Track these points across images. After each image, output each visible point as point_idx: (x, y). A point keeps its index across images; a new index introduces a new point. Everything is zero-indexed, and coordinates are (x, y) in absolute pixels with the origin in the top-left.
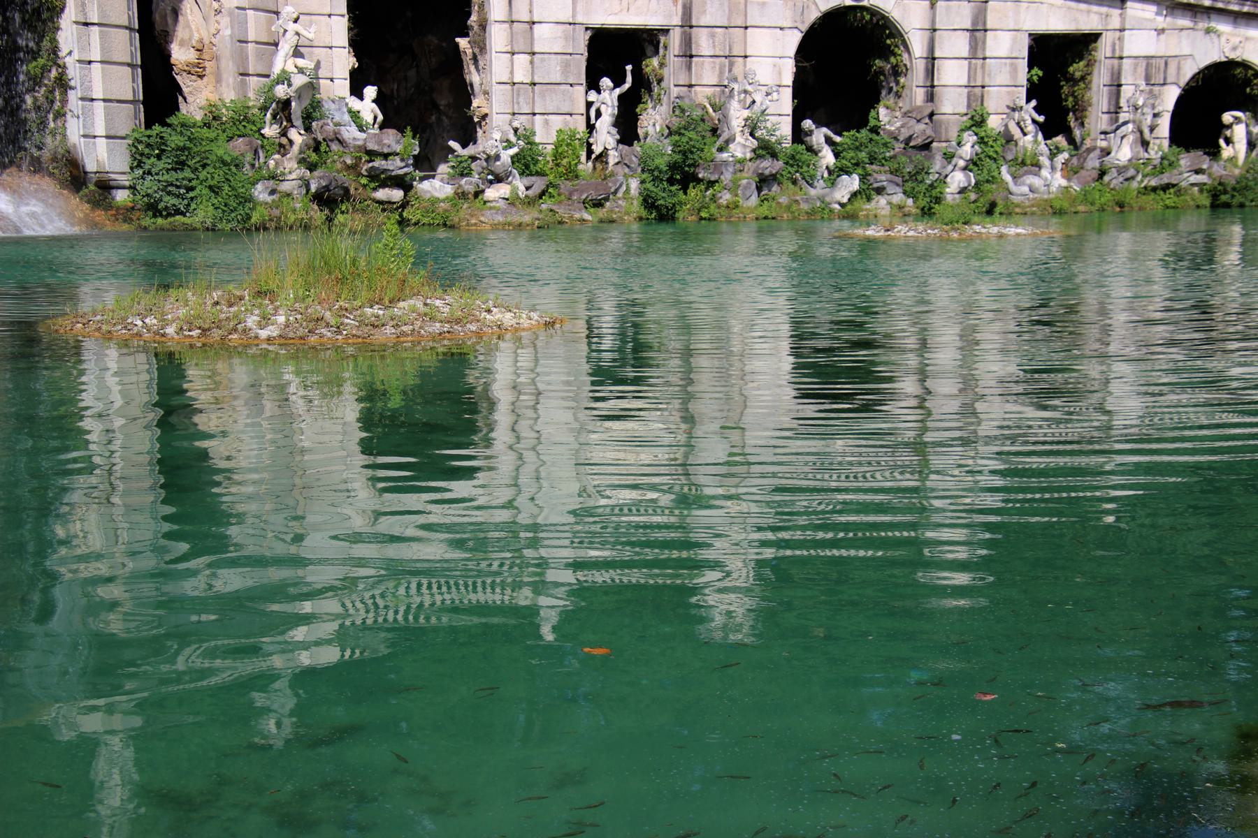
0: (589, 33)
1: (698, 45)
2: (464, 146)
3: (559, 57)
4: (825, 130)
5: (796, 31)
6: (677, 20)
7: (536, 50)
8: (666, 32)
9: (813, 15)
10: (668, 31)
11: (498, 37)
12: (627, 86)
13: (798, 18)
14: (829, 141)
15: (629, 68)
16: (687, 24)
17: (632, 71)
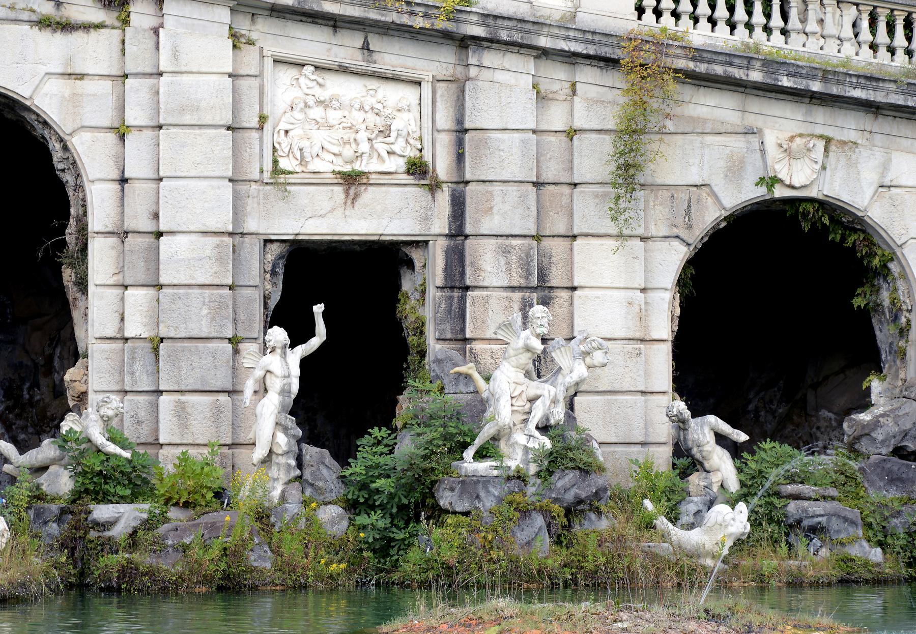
0: (274, 251)
1: (477, 269)
2: (23, 448)
3: (207, 292)
4: (712, 419)
5: (676, 243)
6: (440, 224)
7: (163, 280)
8: (422, 244)
9: (709, 217)
10: (427, 242)
11: (101, 259)
12: (315, 343)
13: (680, 220)
14: (721, 439)
15: (318, 309)
16: (458, 232)
17: (325, 314)
